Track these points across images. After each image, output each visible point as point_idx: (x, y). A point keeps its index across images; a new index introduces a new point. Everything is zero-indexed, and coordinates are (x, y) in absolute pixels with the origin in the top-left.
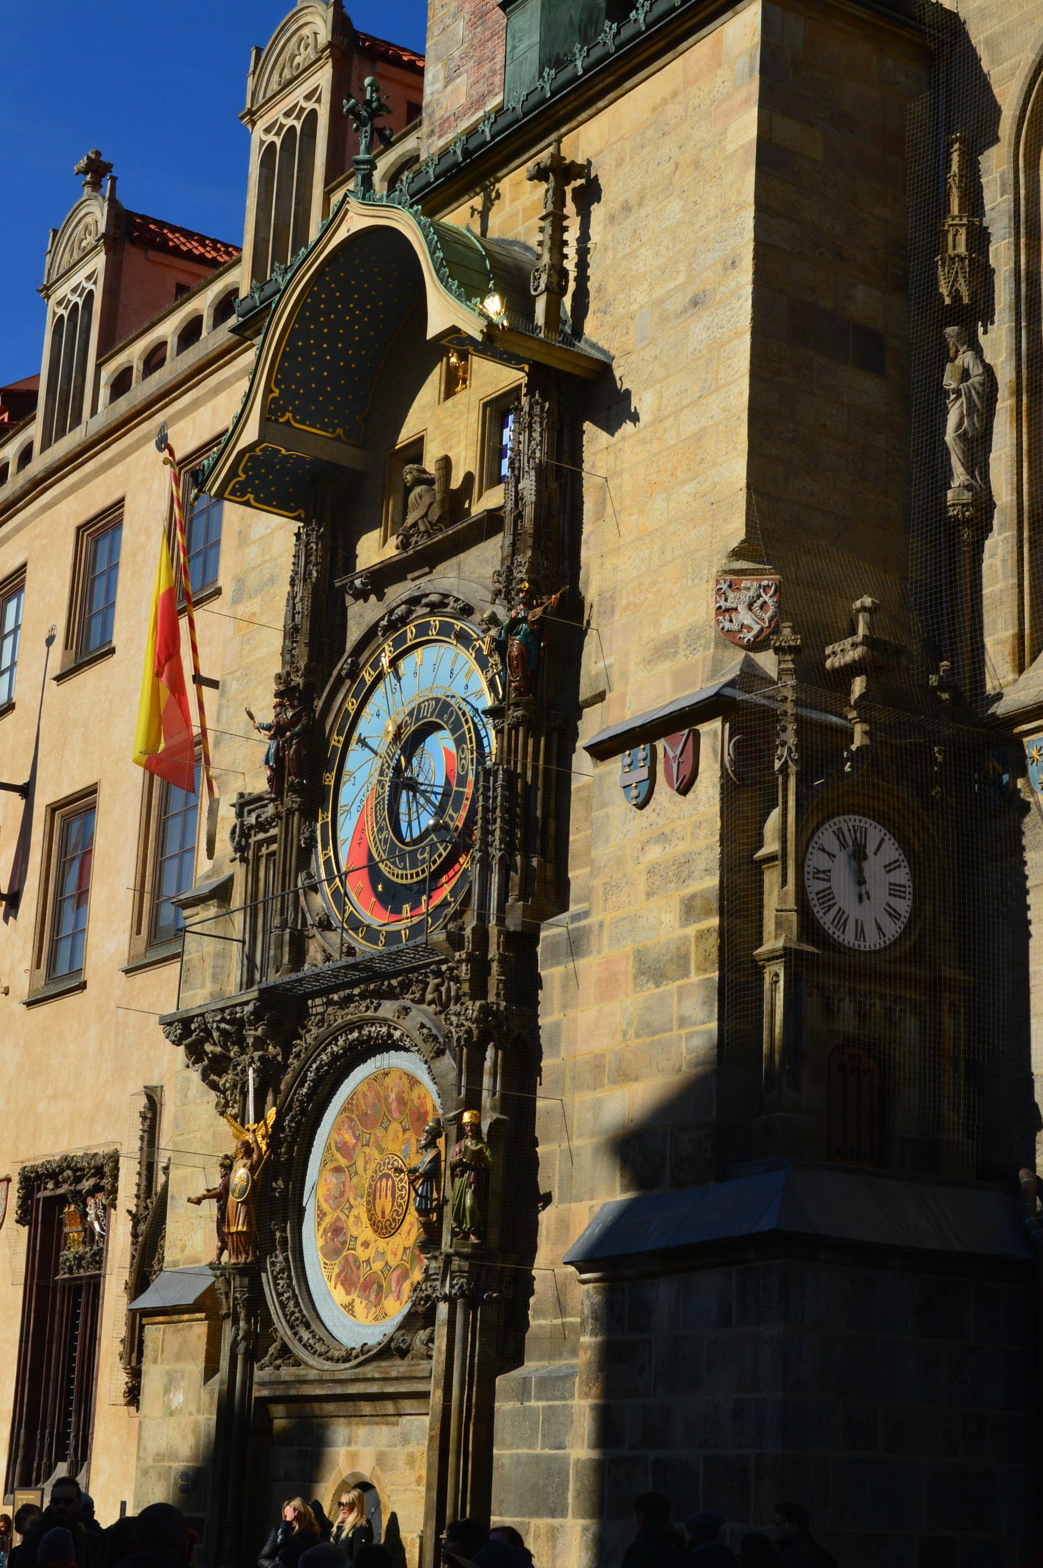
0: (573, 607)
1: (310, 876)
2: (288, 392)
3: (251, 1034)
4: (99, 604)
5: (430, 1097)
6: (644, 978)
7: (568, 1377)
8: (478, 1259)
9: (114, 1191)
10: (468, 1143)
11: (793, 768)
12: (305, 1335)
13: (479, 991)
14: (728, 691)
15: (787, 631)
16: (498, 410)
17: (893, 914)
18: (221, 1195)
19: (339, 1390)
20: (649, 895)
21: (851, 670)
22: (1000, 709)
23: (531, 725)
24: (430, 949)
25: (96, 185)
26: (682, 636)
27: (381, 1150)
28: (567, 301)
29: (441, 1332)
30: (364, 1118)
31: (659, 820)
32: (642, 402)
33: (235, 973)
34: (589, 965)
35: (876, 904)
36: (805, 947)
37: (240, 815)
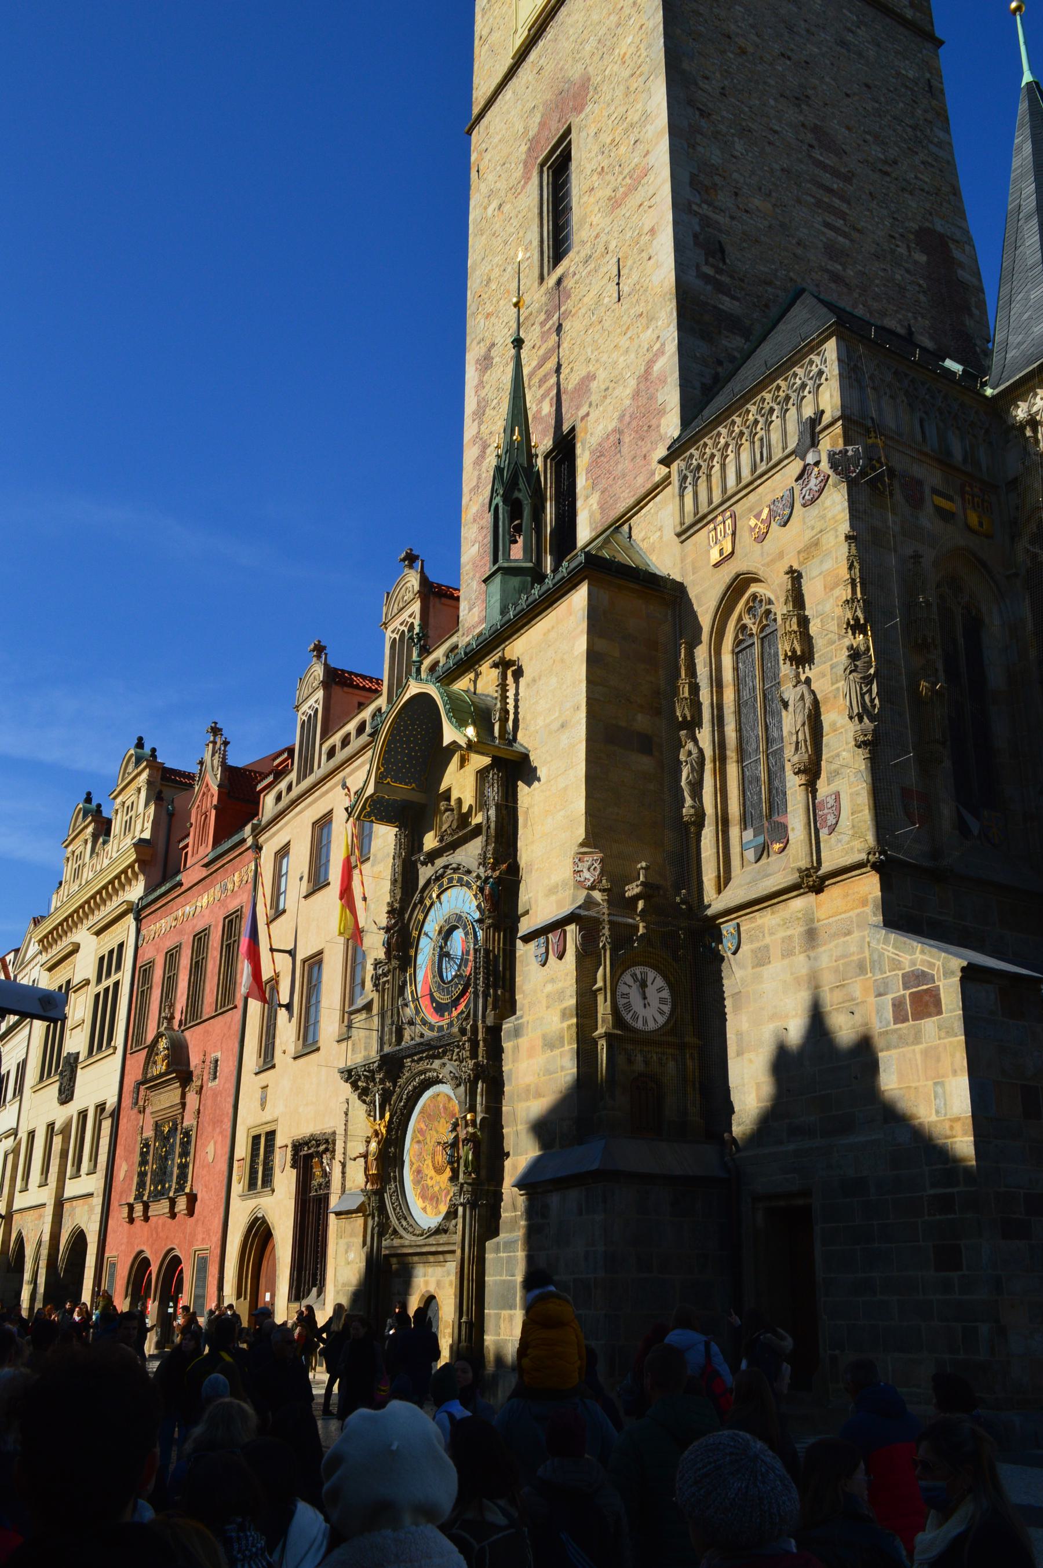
0: (514, 870)
1: (404, 999)
2: (389, 767)
3: (378, 1077)
4: (323, 861)
5: (455, 1106)
7: (516, 1241)
8: (476, 1185)
9: (334, 1151)
10: (470, 1130)
11: (608, 947)
12: (404, 1223)
13: (474, 1055)
14: (578, 911)
15: (604, 881)
16: (482, 774)
17: (662, 1013)
18: (365, 1156)
19: (418, 1250)
20: (548, 1007)
21: (636, 898)
22: (709, 912)
23: (496, 927)
24: (450, 1035)
25: (319, 657)
27: (437, 1132)
28: (510, 723)
29: (460, 1220)
30: (428, 1116)
32: (541, 772)
33: (375, 1046)
34: (523, 1041)
35: (652, 1006)
36: (616, 1031)
37: (375, 969)
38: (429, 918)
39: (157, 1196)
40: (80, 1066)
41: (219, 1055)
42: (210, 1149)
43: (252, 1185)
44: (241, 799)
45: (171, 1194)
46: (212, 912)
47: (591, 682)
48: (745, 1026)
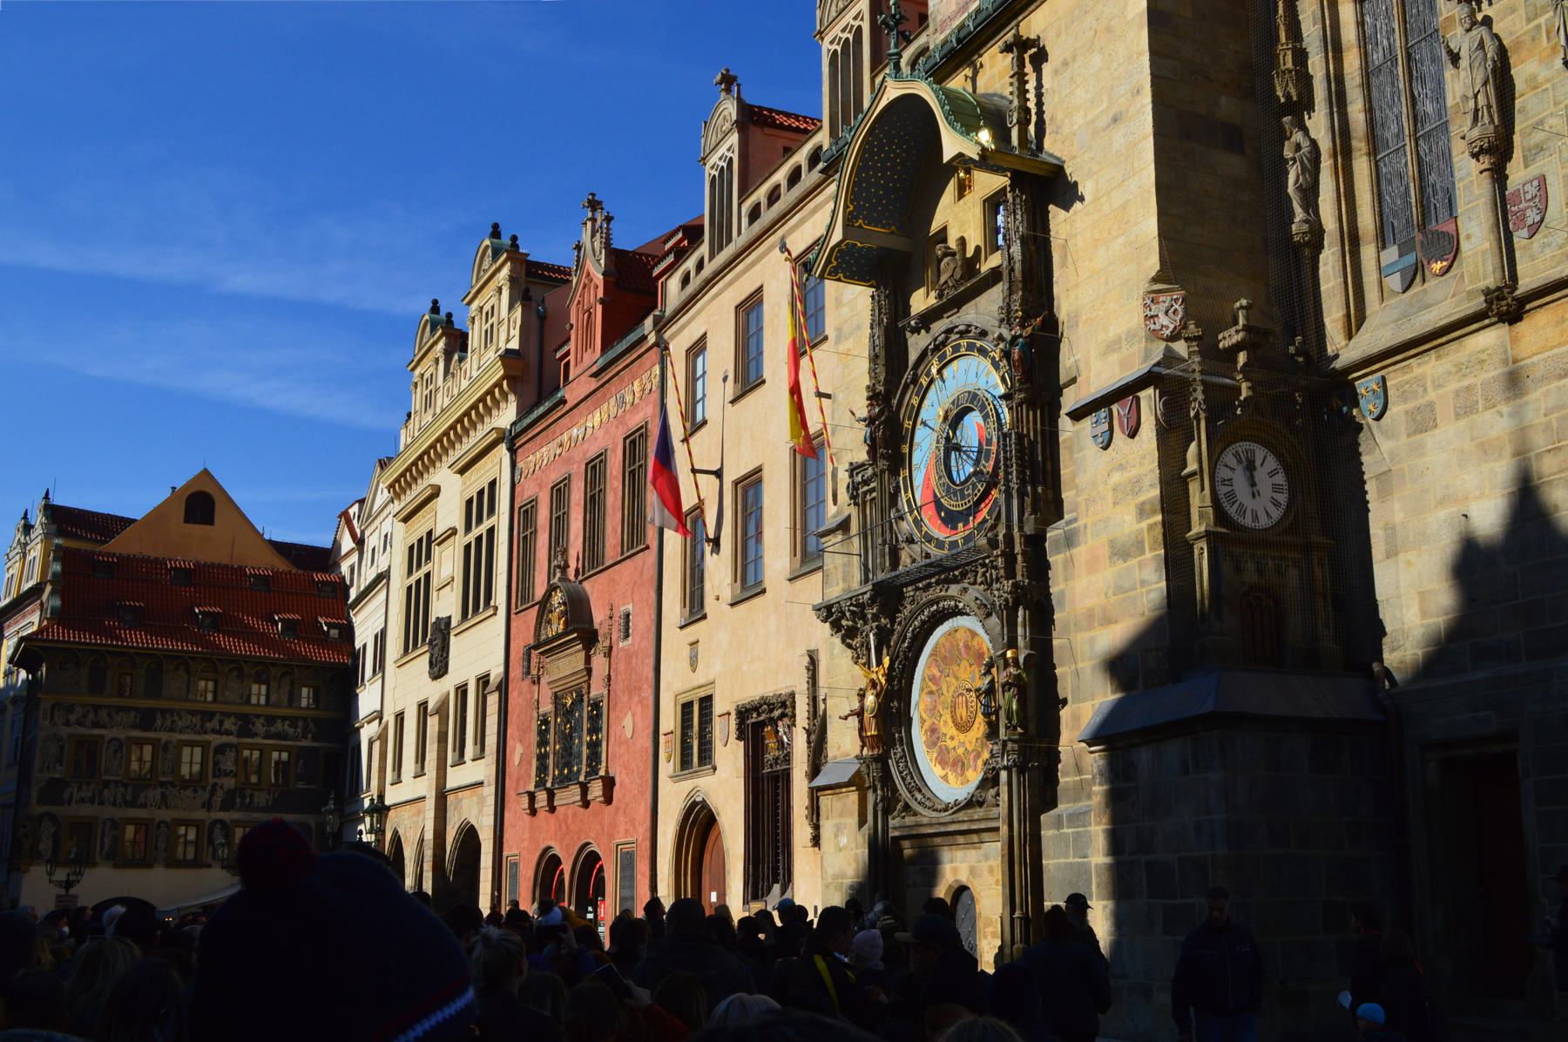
2: (858, 208)
3: (869, 612)
4: (753, 354)
5: (985, 643)
7: (1086, 813)
8: (1023, 742)
9: (794, 716)
11: (1202, 415)
12: (919, 797)
13: (1010, 574)
14: (1156, 369)
16: (993, 204)
18: (860, 713)
19: (943, 829)
20: (1115, 504)
21: (1237, 348)
22: (1338, 364)
23: (1031, 403)
24: (978, 550)
25: (728, 90)
27: (957, 679)
28: (1032, 128)
29: (1004, 789)
30: (945, 659)
33: (857, 575)
34: (1080, 552)
35: (1263, 498)
37: (851, 476)
38: (926, 402)
39: (564, 781)
40: (453, 633)
41: (630, 607)
42: (628, 722)
43: (685, 763)
44: (633, 291)
45: (582, 779)
46: (607, 432)
47: (1157, 53)
48: (1399, 517)
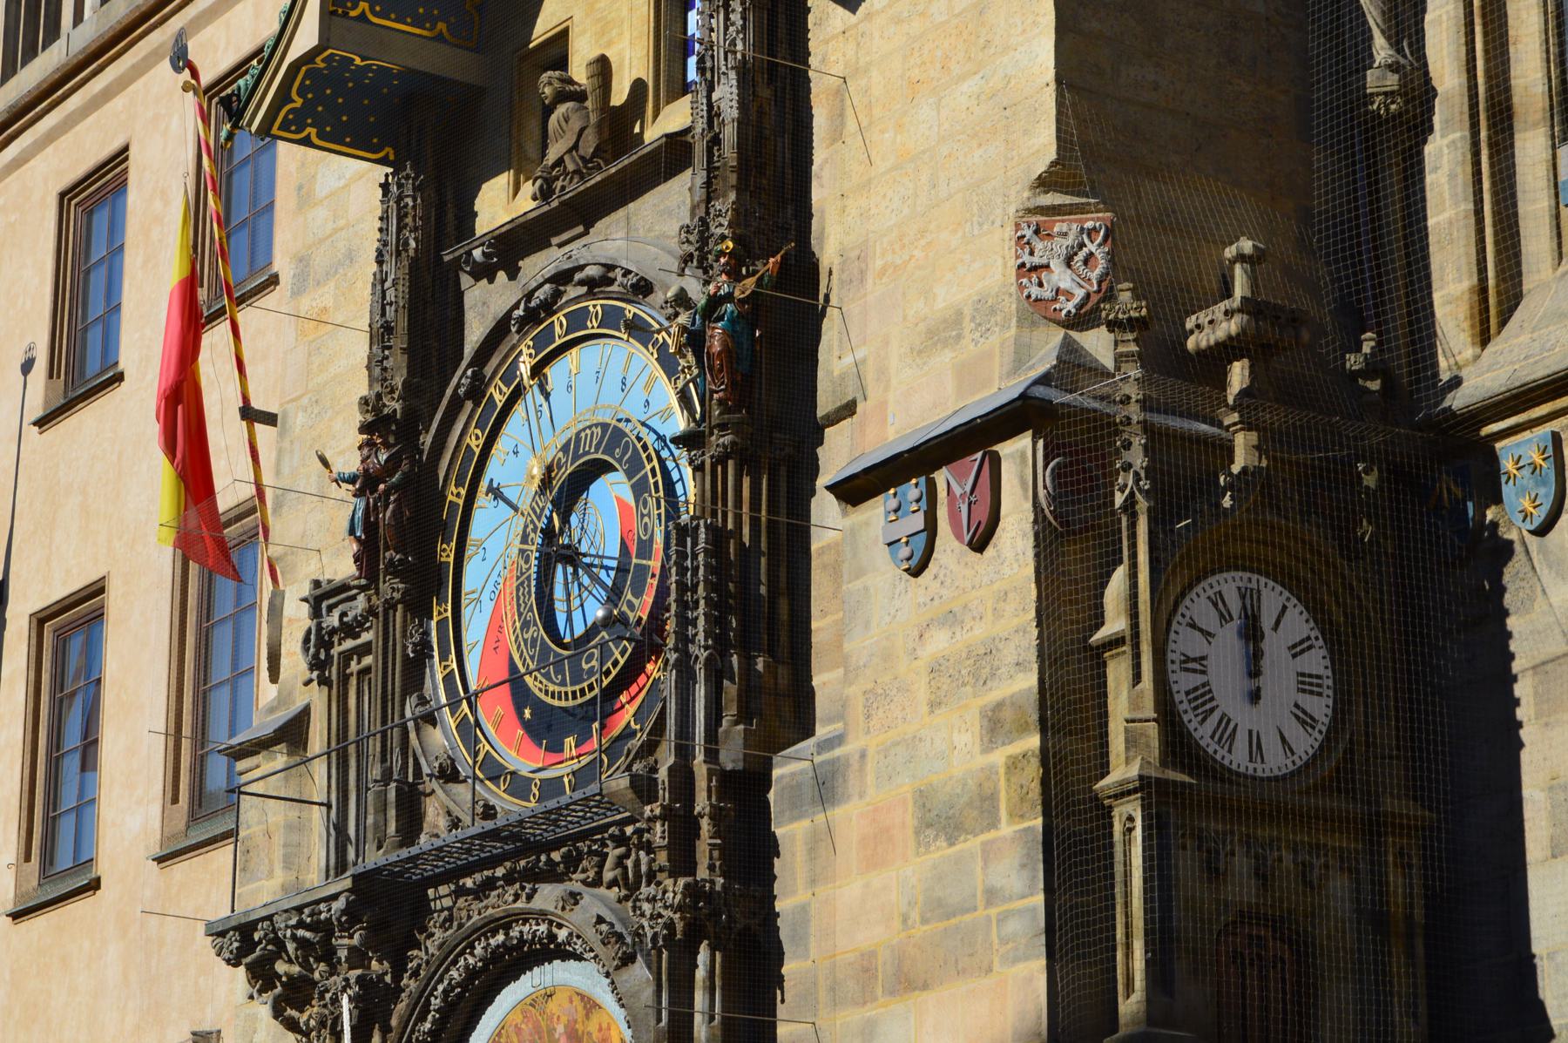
0: (802, 273)
1: (423, 701)
3: (343, 945)
4: (97, 308)
6: (931, 833)
11: (1142, 504)
13: (683, 862)
14: (1040, 391)
15: (1125, 297)
20: (934, 705)
22: (1458, 401)
23: (745, 457)
24: (606, 802)
26: (967, 311)
31: (944, 592)
33: (318, 853)
34: (848, 816)
35: (1277, 709)
37: (316, 613)
38: (502, 445)
